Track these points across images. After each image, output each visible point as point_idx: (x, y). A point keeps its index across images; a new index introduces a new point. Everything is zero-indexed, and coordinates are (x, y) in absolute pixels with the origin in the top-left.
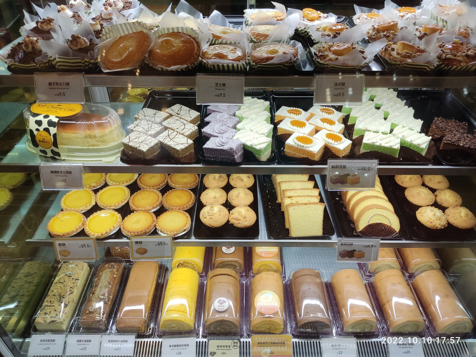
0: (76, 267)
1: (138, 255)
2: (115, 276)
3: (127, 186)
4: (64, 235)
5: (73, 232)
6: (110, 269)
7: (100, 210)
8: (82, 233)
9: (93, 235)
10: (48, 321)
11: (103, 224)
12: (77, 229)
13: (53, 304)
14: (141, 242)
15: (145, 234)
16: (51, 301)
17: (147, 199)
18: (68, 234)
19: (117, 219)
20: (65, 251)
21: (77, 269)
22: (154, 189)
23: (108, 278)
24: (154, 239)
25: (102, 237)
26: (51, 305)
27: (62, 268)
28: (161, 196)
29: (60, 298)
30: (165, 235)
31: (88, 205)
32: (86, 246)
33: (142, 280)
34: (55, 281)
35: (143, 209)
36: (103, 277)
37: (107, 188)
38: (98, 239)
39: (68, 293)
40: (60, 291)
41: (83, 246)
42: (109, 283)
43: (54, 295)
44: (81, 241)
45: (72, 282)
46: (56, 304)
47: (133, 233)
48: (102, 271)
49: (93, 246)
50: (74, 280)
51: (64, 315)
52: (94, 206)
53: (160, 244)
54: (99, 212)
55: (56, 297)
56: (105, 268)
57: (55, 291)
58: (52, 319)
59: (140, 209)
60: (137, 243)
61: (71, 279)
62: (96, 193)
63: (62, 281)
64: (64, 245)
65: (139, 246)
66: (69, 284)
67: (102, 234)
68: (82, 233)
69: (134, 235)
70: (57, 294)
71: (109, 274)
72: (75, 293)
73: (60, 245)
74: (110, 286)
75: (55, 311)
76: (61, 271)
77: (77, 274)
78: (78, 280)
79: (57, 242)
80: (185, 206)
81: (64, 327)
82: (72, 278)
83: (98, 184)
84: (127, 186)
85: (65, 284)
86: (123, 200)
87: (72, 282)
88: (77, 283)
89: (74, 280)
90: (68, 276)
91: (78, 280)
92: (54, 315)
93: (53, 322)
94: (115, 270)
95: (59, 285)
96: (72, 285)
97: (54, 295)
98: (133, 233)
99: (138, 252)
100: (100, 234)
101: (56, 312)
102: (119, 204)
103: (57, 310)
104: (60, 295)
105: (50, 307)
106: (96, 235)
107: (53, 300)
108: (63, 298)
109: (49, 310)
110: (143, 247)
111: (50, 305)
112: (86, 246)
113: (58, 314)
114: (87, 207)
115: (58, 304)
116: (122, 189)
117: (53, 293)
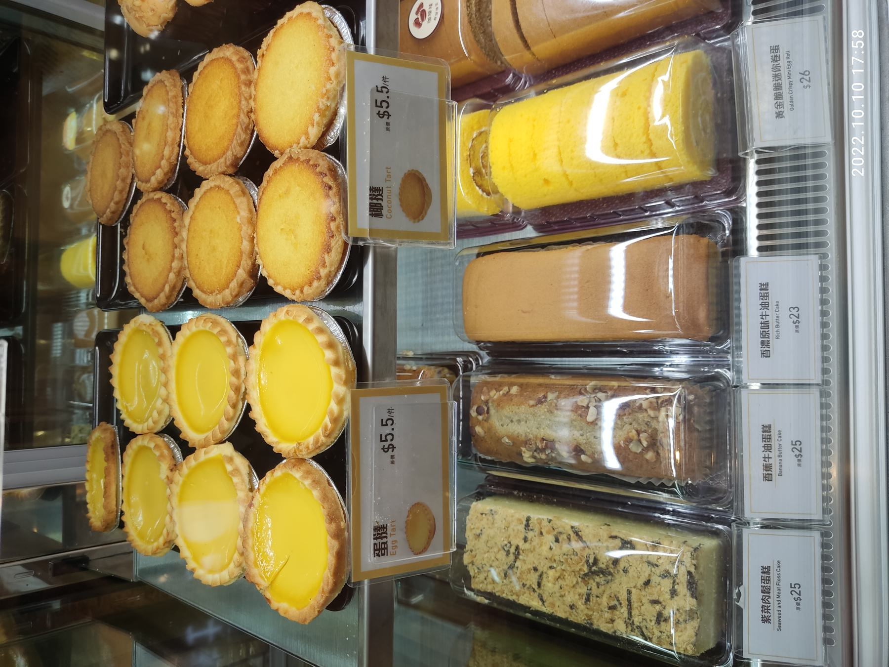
0: (484, 537)
1: (434, 211)
2: (514, 390)
3: (261, 476)
4: (338, 535)
5: (325, 498)
6: (492, 411)
7: (253, 423)
8: (334, 460)
9: (340, 401)
10: (689, 603)
11: (298, 381)
12: (316, 483)
13: (623, 596)
14: (376, 193)
15: (342, 191)
16: (612, 608)
17: (213, 236)
18: (332, 518)
19: (281, 324)
20: (410, 527)
21: (491, 532)
22: (182, 226)
23: (523, 408)
24: (361, 151)
25: (351, 364)
26: (625, 603)
27: (489, 589)
28: (205, 185)
29: (596, 573)
30: (345, 102)
31: (229, 468)
32: (387, 430)
33: (526, 296)
34: (535, 604)
35: (246, 230)
36: (520, 430)
37: (182, 423)
38: (361, 375)
39: (576, 545)
40: (570, 580)
41: (388, 445)
42: (540, 402)
43: (588, 600)
44: (367, 459)
45: (536, 541)
46: (620, 585)
47: (333, 226)
48: (499, 439)
49: (387, 401)
50: (530, 535)
51: (665, 544)
52: (237, 448)
53: (382, 109)
54: (262, 426)
55: (595, 591)
56: (489, 430)
57: (571, 597)
58: (682, 589)
59: (246, 245)
60: (376, 210)
61: (527, 546)
62: (192, 450)
63: (533, 579)
64: (380, 531)
65: (391, 202)
66: (545, 548)
67: (336, 363)
68: (334, 460)
69: (340, 220)
70: (583, 590)
71: (507, 411)
72: (576, 524)
73: (380, 550)
74: (551, 396)
75: (647, 583)
76: (497, 591)
77: (507, 528)
78: (528, 519)
79: (370, 561)
80: (239, 66)
81: (709, 544)
82: (522, 545)
83: (162, 456)
84: (261, 476)
85: (543, 566)
86: (223, 339)
87: (536, 541)
88: (540, 521)
89: (530, 535)
90: (516, 558)
91: (528, 519)
92: (667, 584)
93: (692, 584)
94: (494, 395)
95: (549, 585)
96: (549, 538)
97: (588, 600)
98: (333, 226)
99: (418, 212)
100: (334, 370)
101: (655, 579)
102: (229, 343)
103: (643, 579)
104: (585, 577)
105: (635, 605)
106: (341, 389)
107: (604, 600)
108: (596, 561)
109: (647, 607)
110: (395, 185)
111: (624, 610)
112: (387, 430)
113: (658, 571)
114: (236, 471)
115: (620, 578)
116: (181, 355)
117: (580, 605)
